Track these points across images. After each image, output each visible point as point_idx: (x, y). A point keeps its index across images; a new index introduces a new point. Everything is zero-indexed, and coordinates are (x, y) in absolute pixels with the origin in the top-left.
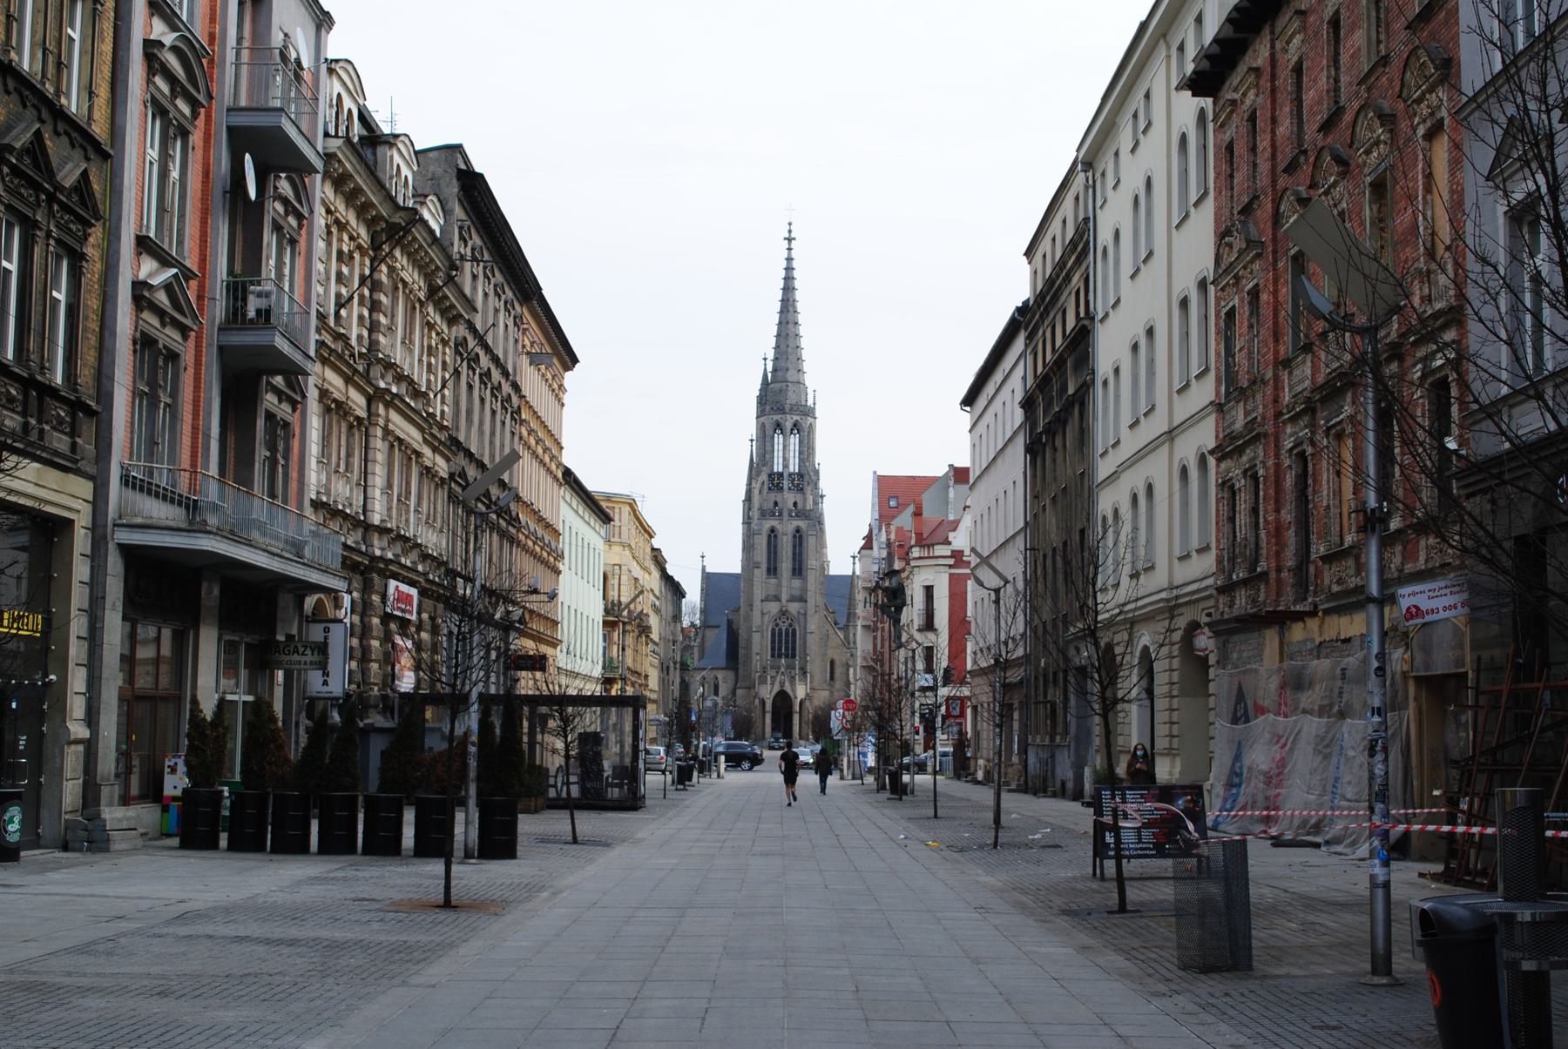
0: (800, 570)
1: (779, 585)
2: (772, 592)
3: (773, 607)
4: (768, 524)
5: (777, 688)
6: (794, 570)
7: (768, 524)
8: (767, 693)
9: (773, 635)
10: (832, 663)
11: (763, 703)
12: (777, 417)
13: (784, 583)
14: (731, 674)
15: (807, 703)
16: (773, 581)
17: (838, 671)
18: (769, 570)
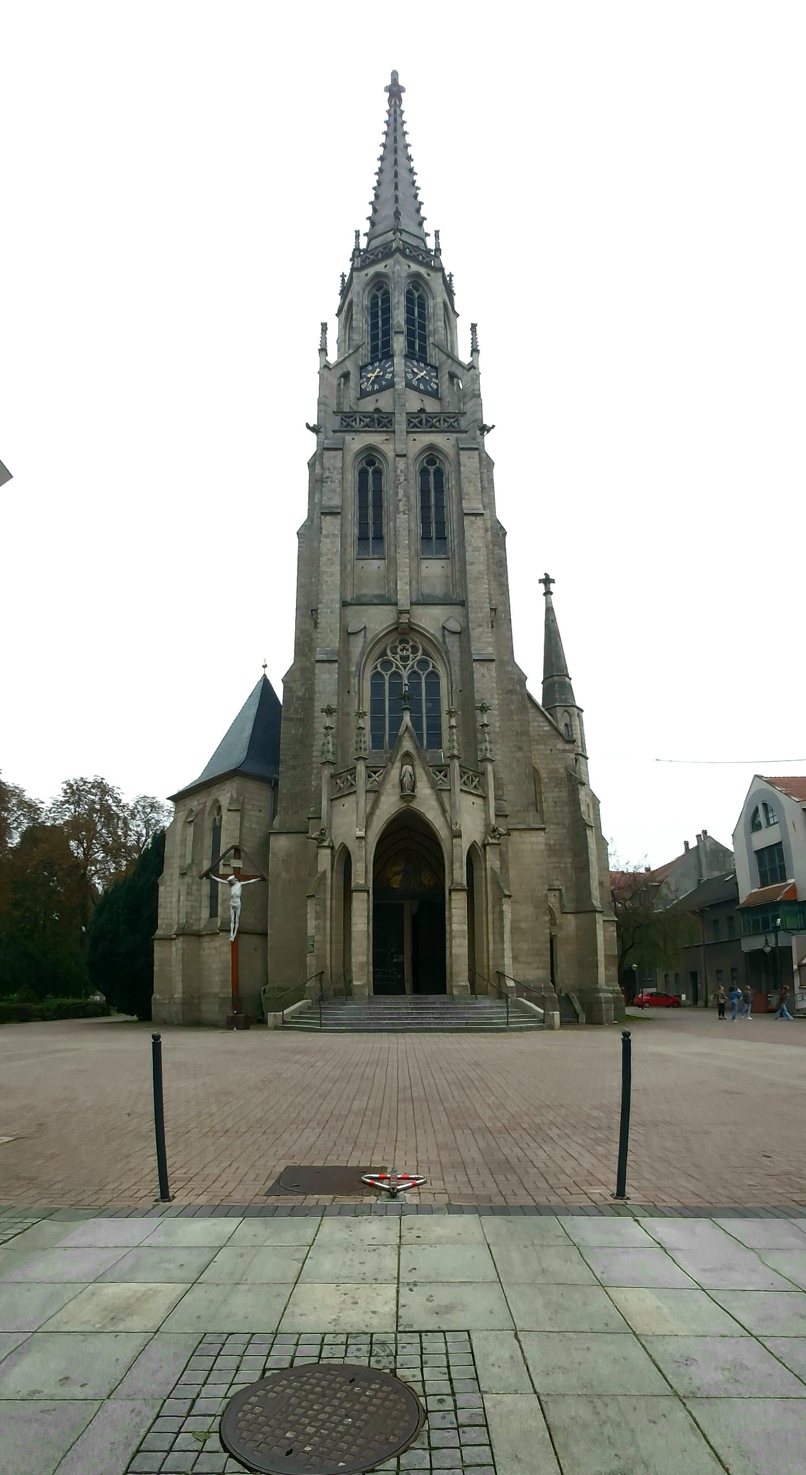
0: (442, 537)
1: (392, 565)
2: (372, 590)
3: (378, 620)
4: (357, 442)
6: (426, 537)
7: (357, 442)
8: (355, 824)
9: (377, 689)
11: (344, 859)
12: (380, 267)
13: (403, 558)
14: (258, 795)
15: (492, 860)
16: (374, 566)
17: (551, 796)
18: (363, 538)
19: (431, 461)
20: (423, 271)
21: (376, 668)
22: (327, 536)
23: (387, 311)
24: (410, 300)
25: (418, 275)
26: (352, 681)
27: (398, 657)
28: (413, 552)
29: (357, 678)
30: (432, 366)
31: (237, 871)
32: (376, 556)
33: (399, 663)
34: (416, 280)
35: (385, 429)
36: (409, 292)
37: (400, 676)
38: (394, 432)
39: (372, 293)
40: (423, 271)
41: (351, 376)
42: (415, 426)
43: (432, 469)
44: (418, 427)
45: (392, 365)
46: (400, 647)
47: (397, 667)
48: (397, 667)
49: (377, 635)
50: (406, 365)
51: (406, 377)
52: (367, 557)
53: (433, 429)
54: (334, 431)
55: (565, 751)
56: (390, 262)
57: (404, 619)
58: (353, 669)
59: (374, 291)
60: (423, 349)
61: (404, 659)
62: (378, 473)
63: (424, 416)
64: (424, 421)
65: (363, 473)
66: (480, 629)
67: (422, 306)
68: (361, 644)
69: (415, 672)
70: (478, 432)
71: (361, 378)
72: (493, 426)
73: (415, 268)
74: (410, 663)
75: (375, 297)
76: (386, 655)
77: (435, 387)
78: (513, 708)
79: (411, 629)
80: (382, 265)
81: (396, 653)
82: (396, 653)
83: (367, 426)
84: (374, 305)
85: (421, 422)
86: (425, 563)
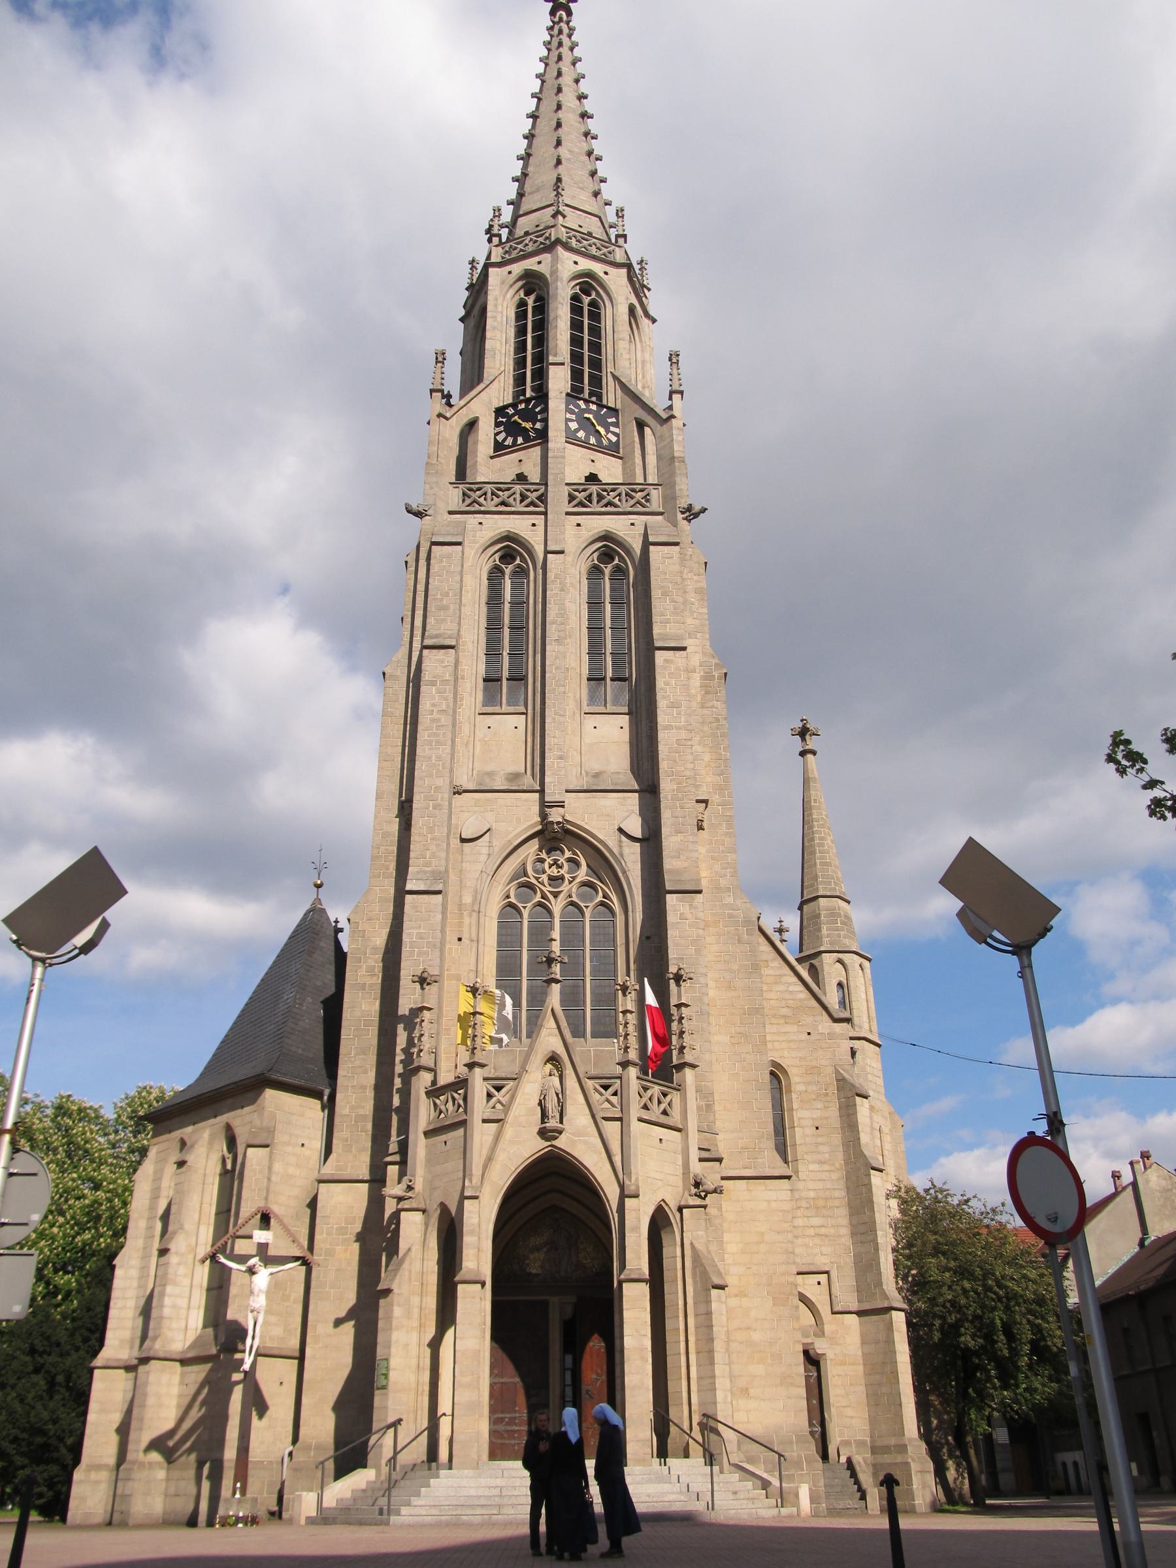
5: (519, 1147)
6: (596, 679)
10: (777, 1074)
12: (530, 264)
15: (693, 1230)
19: (607, 555)
20: (598, 268)
21: (508, 897)
22: (433, 683)
23: (541, 325)
24: (576, 310)
25: (589, 274)
26: (467, 920)
27: (544, 878)
28: (571, 706)
29: (475, 915)
30: (609, 408)
31: (263, 1248)
32: (511, 709)
33: (547, 889)
34: (587, 283)
35: (531, 509)
36: (575, 298)
37: (550, 912)
38: (545, 514)
39: (517, 298)
40: (598, 268)
41: (481, 423)
42: (581, 504)
43: (607, 570)
44: (584, 506)
45: (545, 410)
46: (549, 861)
47: (544, 896)
48: (544, 896)
49: (510, 842)
50: (568, 410)
51: (567, 426)
52: (497, 709)
53: (609, 509)
54: (450, 513)
55: (831, 1036)
56: (546, 257)
57: (555, 815)
58: (467, 899)
59: (522, 293)
60: (596, 381)
61: (556, 880)
62: (521, 572)
63: (594, 489)
64: (595, 495)
65: (495, 575)
66: (679, 837)
67: (595, 316)
68: (483, 858)
69: (573, 904)
70: (680, 516)
71: (497, 424)
72: (704, 510)
73: (585, 264)
74: (565, 887)
75: (522, 304)
76: (526, 875)
77: (614, 439)
78: (735, 967)
79: (568, 832)
80: (537, 259)
81: (544, 872)
82: (544, 872)
83: (503, 503)
84: (521, 315)
85: (590, 496)
86: (591, 721)
